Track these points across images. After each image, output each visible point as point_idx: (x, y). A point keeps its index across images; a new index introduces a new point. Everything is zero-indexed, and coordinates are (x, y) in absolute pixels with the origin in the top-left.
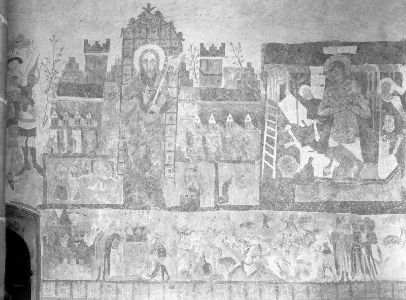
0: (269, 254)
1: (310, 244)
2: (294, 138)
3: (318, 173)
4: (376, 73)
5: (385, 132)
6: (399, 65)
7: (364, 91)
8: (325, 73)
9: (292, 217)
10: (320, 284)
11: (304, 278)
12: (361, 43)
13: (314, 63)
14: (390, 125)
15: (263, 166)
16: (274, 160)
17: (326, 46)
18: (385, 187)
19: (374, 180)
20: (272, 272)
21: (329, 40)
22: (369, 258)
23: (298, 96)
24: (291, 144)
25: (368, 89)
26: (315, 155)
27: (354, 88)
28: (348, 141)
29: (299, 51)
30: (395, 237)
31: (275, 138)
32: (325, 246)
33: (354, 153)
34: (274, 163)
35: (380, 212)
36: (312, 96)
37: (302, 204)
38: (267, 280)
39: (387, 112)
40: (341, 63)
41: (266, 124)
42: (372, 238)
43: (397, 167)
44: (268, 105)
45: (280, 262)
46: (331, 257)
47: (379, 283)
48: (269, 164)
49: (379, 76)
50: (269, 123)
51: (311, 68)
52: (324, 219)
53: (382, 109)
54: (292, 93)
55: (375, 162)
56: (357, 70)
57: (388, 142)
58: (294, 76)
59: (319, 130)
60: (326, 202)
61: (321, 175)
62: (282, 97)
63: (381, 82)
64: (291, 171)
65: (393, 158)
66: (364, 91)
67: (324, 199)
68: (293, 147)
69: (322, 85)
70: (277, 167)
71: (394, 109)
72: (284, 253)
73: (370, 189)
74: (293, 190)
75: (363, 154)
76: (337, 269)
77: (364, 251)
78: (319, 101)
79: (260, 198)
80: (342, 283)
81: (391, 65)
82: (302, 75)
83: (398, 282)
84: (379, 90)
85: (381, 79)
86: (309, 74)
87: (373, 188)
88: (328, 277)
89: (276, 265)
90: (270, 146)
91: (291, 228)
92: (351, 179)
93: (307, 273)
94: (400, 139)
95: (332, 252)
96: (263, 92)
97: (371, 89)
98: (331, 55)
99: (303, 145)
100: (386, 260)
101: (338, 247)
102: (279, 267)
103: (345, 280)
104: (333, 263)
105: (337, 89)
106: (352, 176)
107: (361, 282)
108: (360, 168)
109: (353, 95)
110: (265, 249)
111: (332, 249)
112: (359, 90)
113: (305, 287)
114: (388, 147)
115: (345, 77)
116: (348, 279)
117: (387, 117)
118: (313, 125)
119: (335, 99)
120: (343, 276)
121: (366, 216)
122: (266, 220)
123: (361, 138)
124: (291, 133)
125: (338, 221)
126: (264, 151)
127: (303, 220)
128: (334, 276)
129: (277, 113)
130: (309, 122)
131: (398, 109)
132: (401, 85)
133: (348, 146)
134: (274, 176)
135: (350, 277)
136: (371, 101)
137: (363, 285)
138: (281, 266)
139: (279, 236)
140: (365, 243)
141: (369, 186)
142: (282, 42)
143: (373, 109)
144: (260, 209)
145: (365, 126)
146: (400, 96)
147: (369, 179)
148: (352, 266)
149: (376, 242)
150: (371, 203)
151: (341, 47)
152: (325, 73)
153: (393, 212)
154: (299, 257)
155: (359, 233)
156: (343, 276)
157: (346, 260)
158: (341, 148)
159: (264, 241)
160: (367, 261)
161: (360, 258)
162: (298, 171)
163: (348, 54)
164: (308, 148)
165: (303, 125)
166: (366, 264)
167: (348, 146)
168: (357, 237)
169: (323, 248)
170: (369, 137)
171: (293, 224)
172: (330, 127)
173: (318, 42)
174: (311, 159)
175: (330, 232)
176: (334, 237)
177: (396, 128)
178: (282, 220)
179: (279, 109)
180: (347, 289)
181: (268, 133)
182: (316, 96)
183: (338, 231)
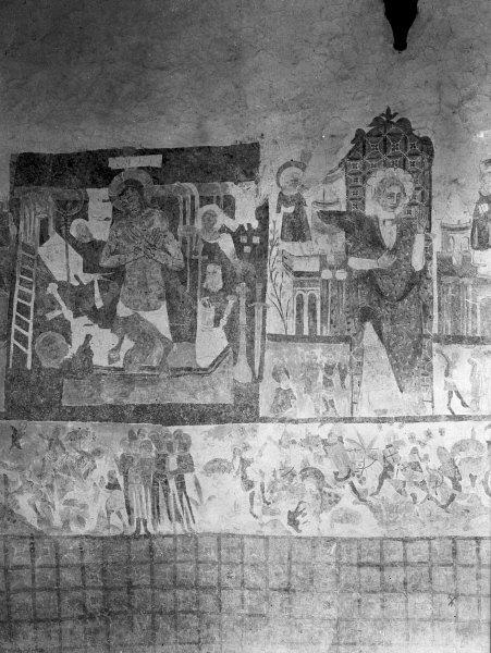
0: (20, 491)
1: (87, 473)
2: (62, 303)
3: (99, 359)
4: (193, 198)
5: (206, 292)
6: (229, 183)
7: (173, 227)
8: (111, 199)
9: (57, 431)
10: (102, 538)
11: (75, 529)
12: (169, 150)
13: (95, 184)
14: (215, 281)
15: (12, 349)
16: (30, 340)
17: (114, 156)
18: (207, 380)
19: (189, 369)
20: (25, 519)
21: (119, 146)
22: (181, 497)
23: (68, 237)
24: (57, 313)
25: (181, 222)
26: (95, 330)
27: (158, 222)
28: (148, 308)
29: (70, 165)
30: (225, 461)
31: (31, 305)
32: (111, 476)
33: (158, 327)
34: (30, 344)
35: (200, 421)
36: (91, 236)
37: (73, 409)
38: (17, 532)
39: (211, 260)
40: (137, 182)
41: (18, 282)
42: (186, 463)
43: (227, 347)
44: (21, 252)
45: (38, 504)
46: (119, 494)
47: (196, 539)
48: (21, 347)
49: (197, 202)
50: (21, 280)
51: (89, 191)
52: (109, 434)
54: (60, 232)
55: (192, 340)
56: (162, 193)
57: (213, 308)
58: (62, 205)
59: (101, 290)
60: (111, 406)
61: (105, 363)
62: (43, 238)
63: (201, 211)
64: (56, 357)
65: (220, 332)
66: (173, 227)
67: (110, 400)
68: (61, 319)
69: (107, 219)
70: (33, 351)
71: (222, 254)
72: (44, 489)
73: (183, 383)
74: (60, 387)
75: (172, 328)
76: (129, 513)
77: (172, 484)
78: (101, 244)
79: (7, 400)
80: (136, 536)
81: (216, 183)
82: (75, 202)
83: (228, 535)
84: (199, 225)
85: (201, 206)
86: (86, 202)
87: (189, 383)
88: (115, 527)
89: (31, 509)
90: (25, 319)
91: (57, 448)
92: (153, 369)
93: (81, 520)
94: (231, 303)
95: (122, 486)
96: (13, 231)
97: (185, 223)
98: (120, 171)
99: (77, 315)
100: (209, 499)
101: (131, 479)
102: (36, 510)
103: (142, 532)
104: (121, 505)
105: (130, 225)
106: (155, 364)
107: (168, 536)
108: (167, 351)
109: (156, 233)
110: (15, 483)
111: (121, 482)
112: (166, 225)
113: (77, 543)
114: (212, 316)
115: (144, 205)
116: (146, 530)
117: (210, 268)
118: (93, 283)
119: (128, 240)
120: (139, 525)
121: (176, 428)
122: (16, 435)
123: (168, 302)
124: (57, 296)
125: (132, 437)
126: (14, 326)
127: (75, 436)
128: (124, 525)
129: (36, 265)
130: (86, 278)
131: (228, 255)
132: (232, 216)
133: (149, 316)
134: (29, 366)
135: (150, 527)
136: (184, 243)
137: (170, 541)
138: (39, 510)
139: (37, 461)
140: (176, 472)
141: (182, 378)
142: (44, 150)
143: (188, 255)
144: (6, 418)
145: (175, 282)
146: (231, 233)
147: (182, 368)
148: (153, 509)
149: (193, 470)
150: (184, 406)
151: (138, 158)
152: (111, 199)
153: (220, 421)
154: (69, 496)
155: (165, 455)
156: (139, 525)
157: (144, 500)
158: (137, 319)
159: (12, 469)
160: (178, 502)
161: (166, 496)
162: (69, 356)
163: (148, 168)
164: (85, 319)
165: (76, 284)
166: (176, 506)
167: (149, 316)
168: (161, 462)
169: (107, 481)
170: (181, 300)
171: (59, 442)
172: (120, 285)
173: (100, 151)
174: (88, 337)
175: (119, 454)
176: (125, 463)
178: (41, 435)
179: (39, 258)
180: (144, 545)
181: (19, 297)
182: (97, 236)
183: (132, 452)
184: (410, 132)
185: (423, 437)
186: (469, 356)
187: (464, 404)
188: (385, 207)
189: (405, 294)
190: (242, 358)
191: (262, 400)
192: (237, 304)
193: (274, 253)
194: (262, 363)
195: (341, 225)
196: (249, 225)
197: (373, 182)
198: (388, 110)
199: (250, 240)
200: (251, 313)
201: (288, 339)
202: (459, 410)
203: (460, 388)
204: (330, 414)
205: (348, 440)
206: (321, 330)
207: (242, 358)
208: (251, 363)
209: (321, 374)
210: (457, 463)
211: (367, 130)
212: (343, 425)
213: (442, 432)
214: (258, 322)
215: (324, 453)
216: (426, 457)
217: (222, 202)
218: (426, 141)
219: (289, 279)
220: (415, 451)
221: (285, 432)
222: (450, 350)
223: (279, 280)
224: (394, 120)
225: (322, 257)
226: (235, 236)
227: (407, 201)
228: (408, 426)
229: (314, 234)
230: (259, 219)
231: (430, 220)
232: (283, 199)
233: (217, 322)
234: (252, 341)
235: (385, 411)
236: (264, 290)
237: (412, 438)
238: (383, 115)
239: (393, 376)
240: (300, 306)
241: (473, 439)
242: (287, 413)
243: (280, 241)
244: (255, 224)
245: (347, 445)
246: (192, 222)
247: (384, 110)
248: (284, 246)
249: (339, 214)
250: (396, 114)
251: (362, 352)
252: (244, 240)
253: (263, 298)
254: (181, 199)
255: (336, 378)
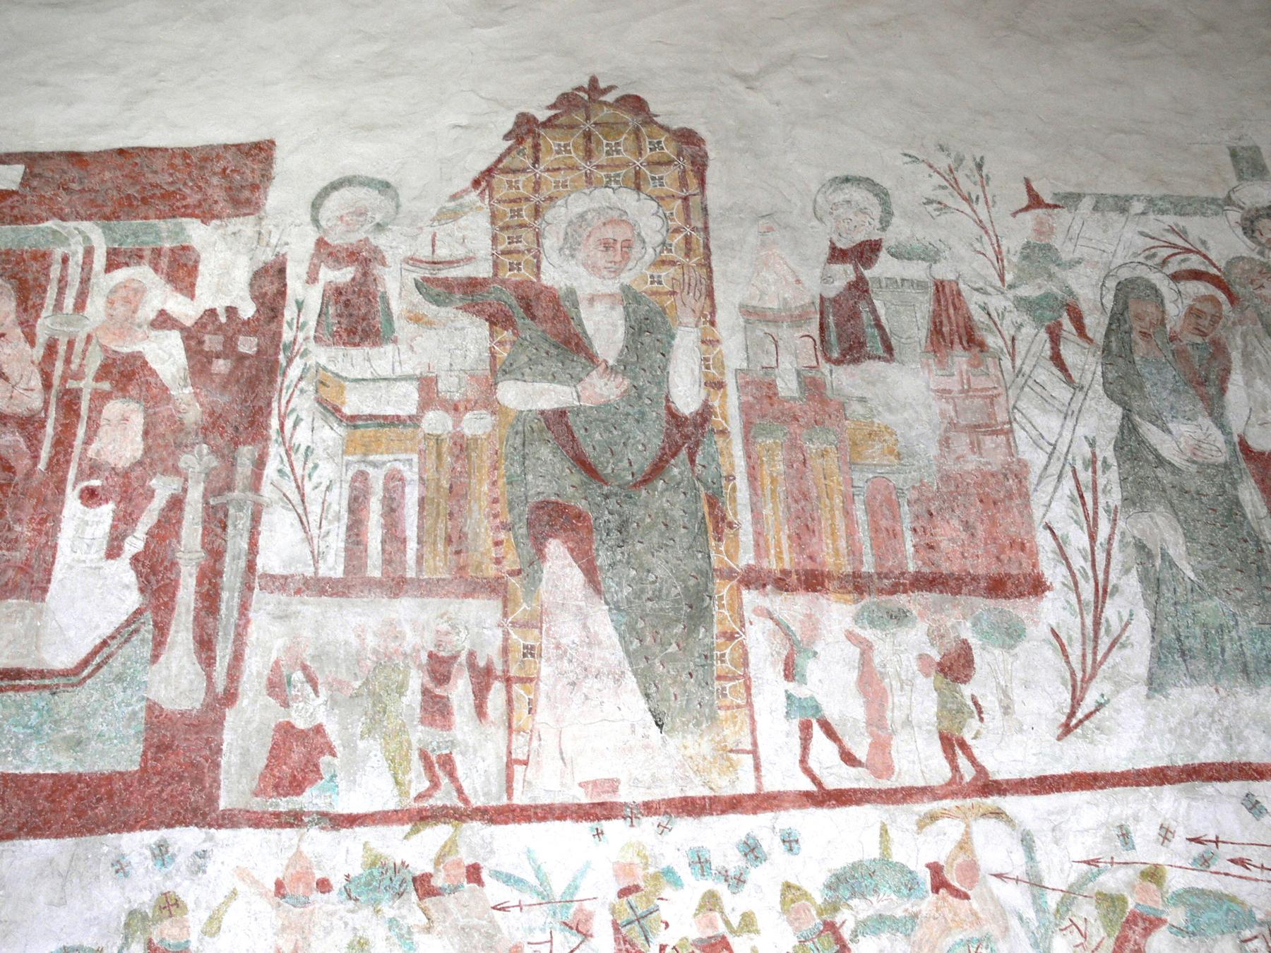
4: (89, 252)
12: (44, 156)
43: (139, 612)
53: (98, 378)
63: (104, 282)
65: (122, 572)
84: (96, 307)
85: (111, 266)
97: (58, 306)
132: (189, 290)
136: (51, 348)
143: (56, 381)
146: (183, 329)
177: (147, 450)
184: (649, 120)
185: (728, 857)
186: (848, 623)
187: (848, 758)
188: (593, 268)
189: (658, 468)
190: (182, 635)
191: (229, 760)
192: (176, 503)
193: (294, 372)
194: (237, 657)
195: (474, 308)
196: (231, 311)
197: (559, 216)
198: (594, 81)
199: (230, 343)
200: (216, 521)
201: (320, 587)
202: (838, 777)
203: (832, 712)
204: (444, 797)
205: (497, 875)
206: (420, 559)
207: (182, 635)
208: (205, 645)
209: (416, 680)
210: (846, 933)
211: (542, 116)
212: (476, 830)
213: (790, 842)
214: (237, 543)
215: (418, 918)
216: (748, 923)
217: (164, 263)
218: (687, 137)
219: (330, 435)
220: (710, 902)
221: (299, 853)
222: (794, 607)
223: (302, 437)
224: (610, 98)
225: (427, 385)
226: (192, 337)
227: (650, 255)
228: (687, 830)
229: (403, 329)
230: (258, 298)
231: (710, 294)
232: (325, 251)
233: (113, 551)
234: (209, 599)
235: (613, 785)
236: (260, 463)
237: (700, 863)
238: (580, 89)
239: (631, 681)
240: (357, 505)
241: (885, 860)
242: (311, 799)
243: (312, 345)
244: (248, 310)
245: (494, 891)
246: (80, 305)
247: (585, 82)
248: (321, 356)
249: (472, 285)
250: (611, 88)
251: (533, 622)
252: (212, 342)
253: (255, 482)
254: (58, 252)
255: (460, 690)
